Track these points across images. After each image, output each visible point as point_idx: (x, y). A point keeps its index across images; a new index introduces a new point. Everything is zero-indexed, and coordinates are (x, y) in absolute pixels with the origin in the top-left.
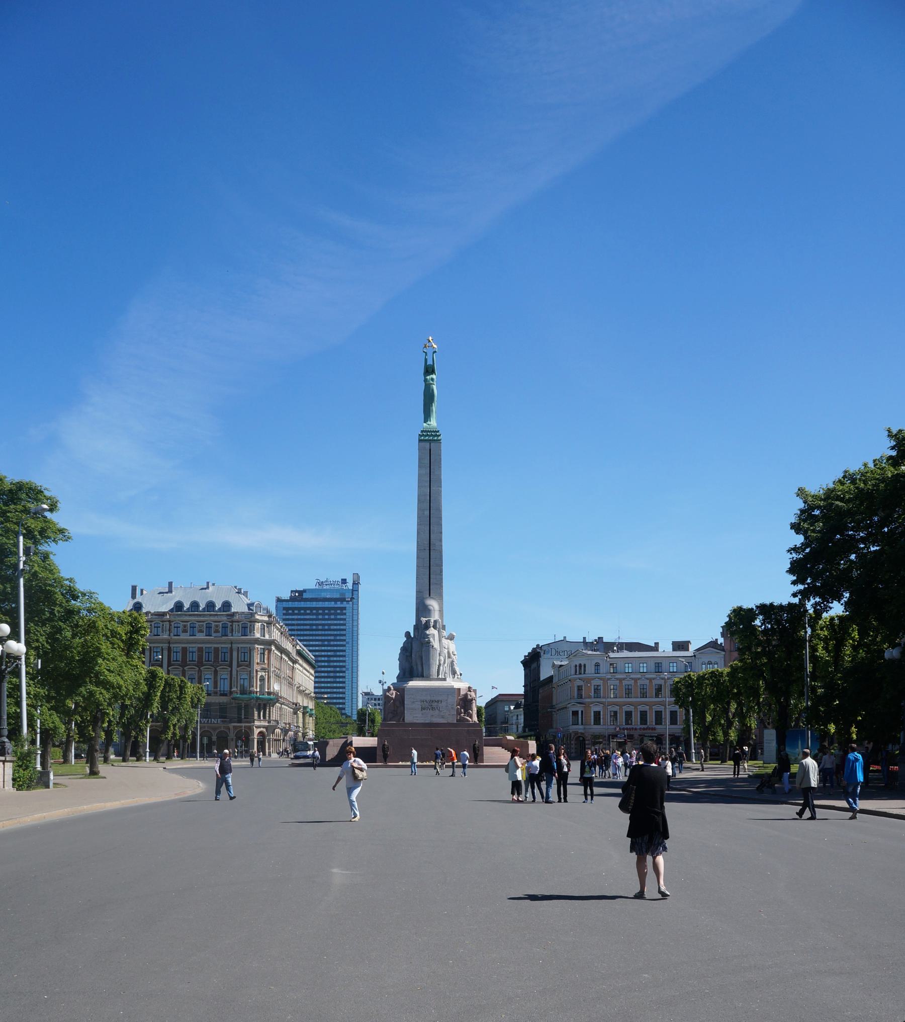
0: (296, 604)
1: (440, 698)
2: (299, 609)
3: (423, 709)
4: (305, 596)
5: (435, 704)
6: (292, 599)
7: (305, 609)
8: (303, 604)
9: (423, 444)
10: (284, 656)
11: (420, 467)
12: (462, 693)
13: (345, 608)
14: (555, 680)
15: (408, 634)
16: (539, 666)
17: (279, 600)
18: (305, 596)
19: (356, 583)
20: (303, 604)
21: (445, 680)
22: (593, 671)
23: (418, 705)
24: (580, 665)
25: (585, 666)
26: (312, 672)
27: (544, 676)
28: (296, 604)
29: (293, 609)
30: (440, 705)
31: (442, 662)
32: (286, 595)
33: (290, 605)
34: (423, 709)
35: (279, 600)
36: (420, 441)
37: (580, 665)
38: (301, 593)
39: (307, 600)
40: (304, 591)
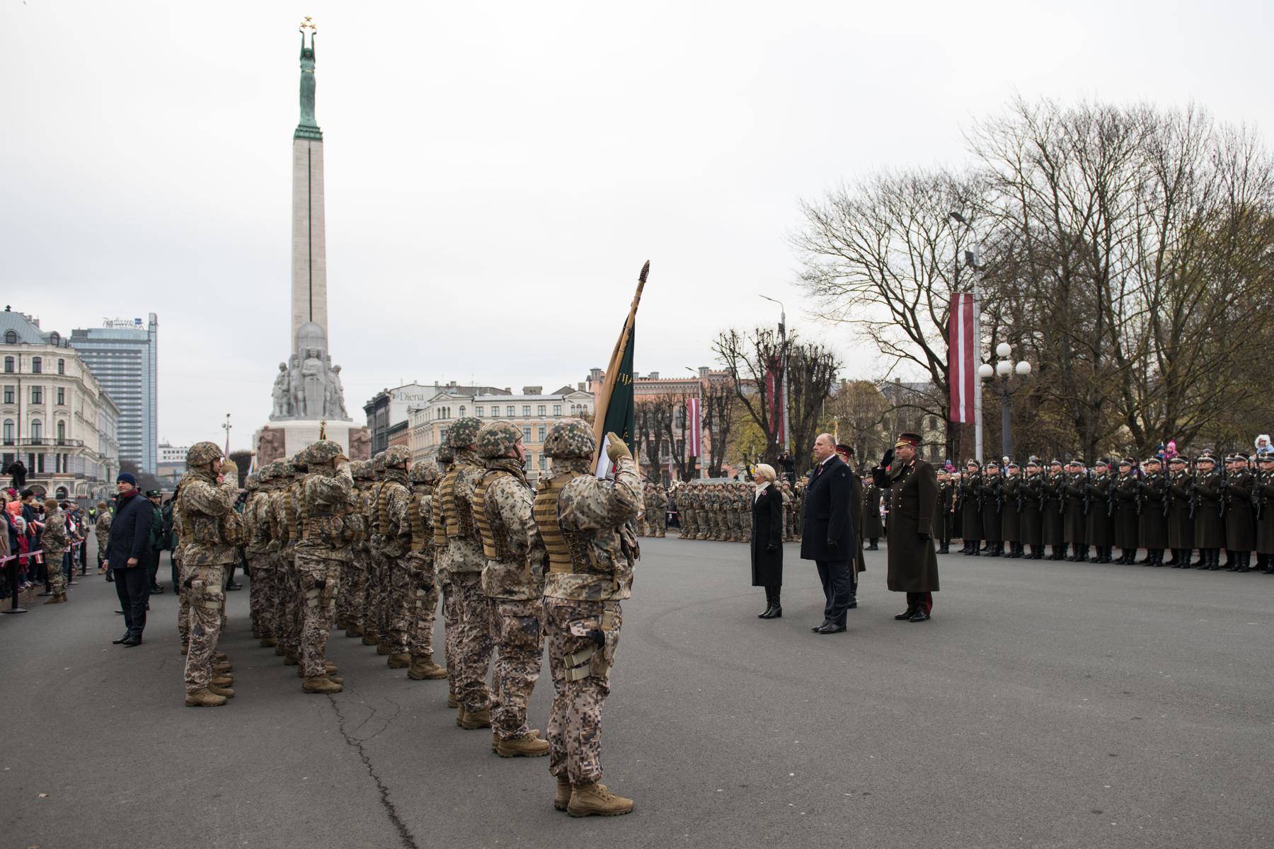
4: (90, 336)
8: (87, 346)
9: (298, 141)
13: (140, 351)
14: (411, 425)
15: (283, 368)
16: (387, 412)
18: (90, 336)
19: (154, 324)
20: (87, 346)
27: (394, 420)
36: (297, 137)
39: (92, 341)
40: (89, 331)
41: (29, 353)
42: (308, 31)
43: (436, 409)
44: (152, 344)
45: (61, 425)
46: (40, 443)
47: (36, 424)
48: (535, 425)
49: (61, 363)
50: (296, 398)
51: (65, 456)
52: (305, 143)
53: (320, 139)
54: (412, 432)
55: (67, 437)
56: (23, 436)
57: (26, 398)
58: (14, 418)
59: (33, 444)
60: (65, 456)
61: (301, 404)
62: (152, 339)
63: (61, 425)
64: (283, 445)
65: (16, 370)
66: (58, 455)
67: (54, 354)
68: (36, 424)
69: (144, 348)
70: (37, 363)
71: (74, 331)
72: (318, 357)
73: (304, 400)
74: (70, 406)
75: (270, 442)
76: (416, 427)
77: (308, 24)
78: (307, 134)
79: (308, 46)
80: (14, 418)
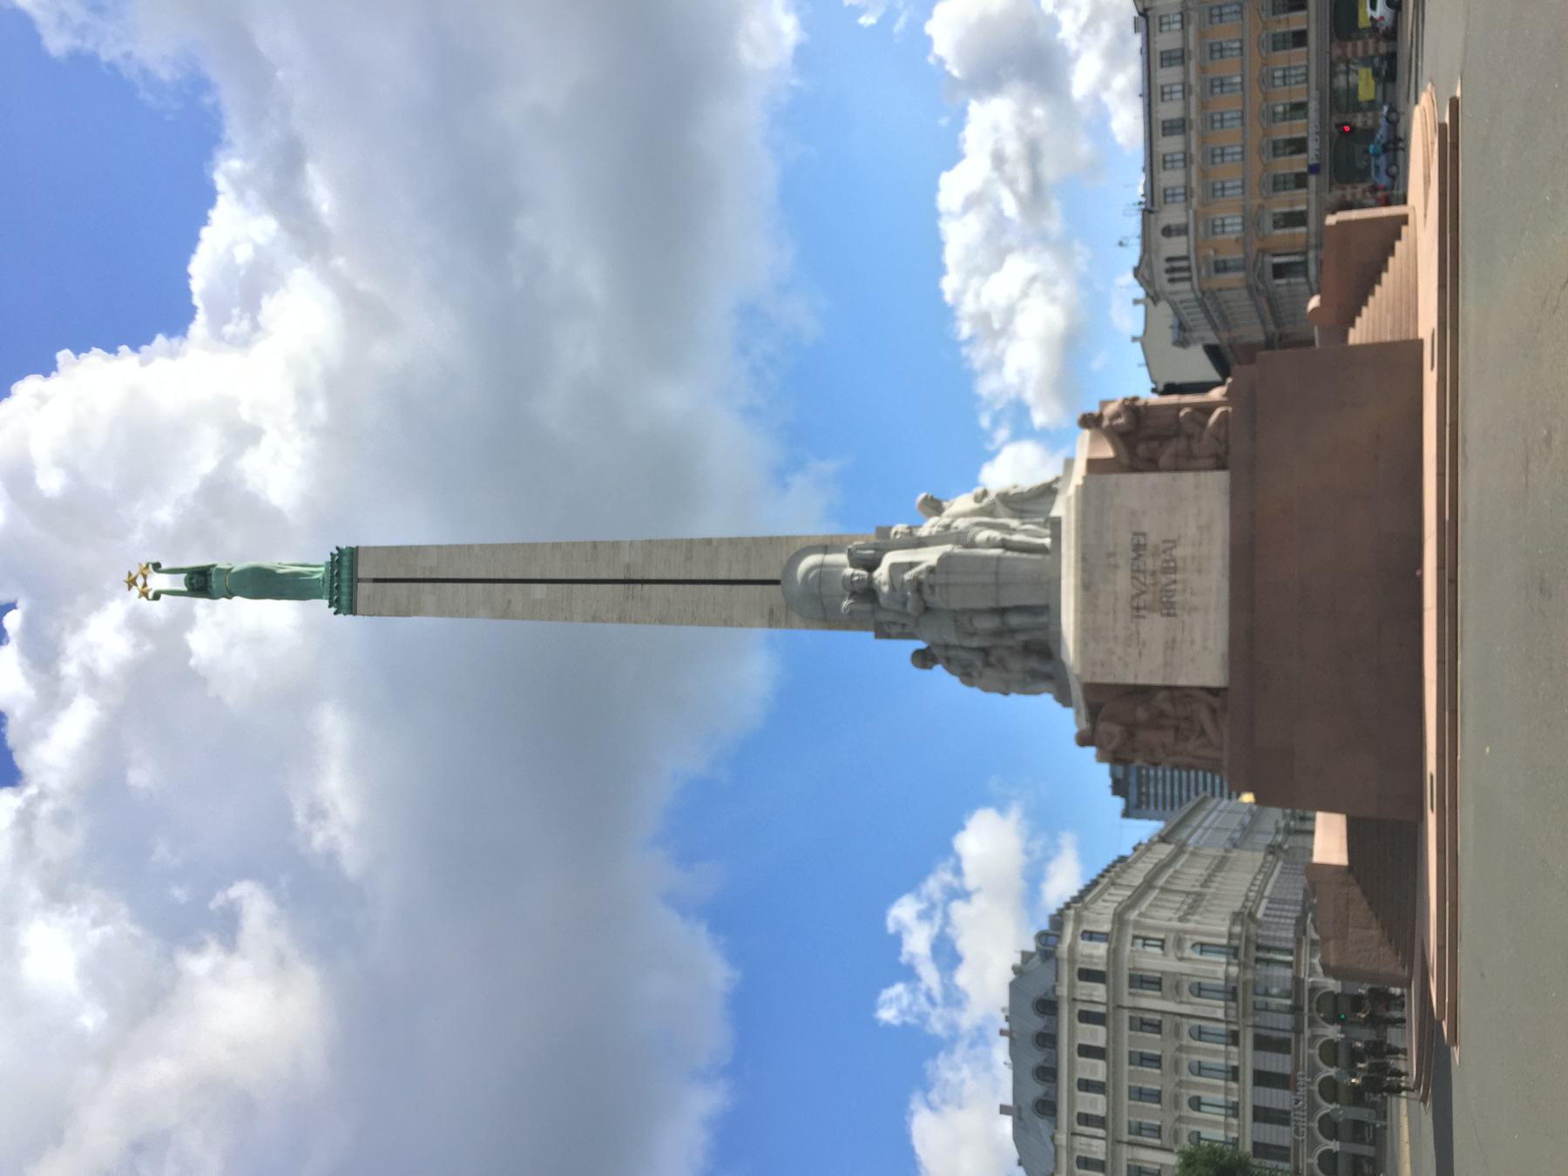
0: (1133, 790)
1: (1125, 539)
10: (1161, 882)
11: (417, 612)
12: (1107, 452)
14: (1212, 339)
15: (924, 659)
17: (1126, 814)
21: (1055, 524)
22: (1183, 239)
23: (1155, 626)
24: (1167, 271)
25: (1169, 259)
26: (1213, 802)
31: (997, 535)
32: (1118, 803)
34: (1168, 608)
35: (1126, 814)
36: (352, 610)
37: (1170, 270)
41: (1072, 987)
42: (158, 582)
43: (1169, 287)
45: (1203, 947)
46: (1235, 989)
47: (1199, 990)
48: (1202, 70)
49: (1090, 936)
50: (998, 633)
51: (1259, 948)
52: (364, 589)
53: (353, 553)
54: (1225, 335)
55: (1224, 941)
56: (1220, 1014)
57: (1151, 1001)
58: (1187, 1024)
59: (1234, 999)
60: (1259, 948)
61: (1014, 620)
63: (1203, 947)
64: (1141, 693)
65: (1101, 1009)
66: (1258, 960)
67: (1072, 949)
68: (1199, 990)
70: (1088, 975)
72: (872, 565)
73: (1002, 612)
74: (1168, 930)
75: (1131, 729)
76: (1215, 328)
77: (140, 581)
78: (345, 589)
79: (179, 583)
80: (1187, 1024)
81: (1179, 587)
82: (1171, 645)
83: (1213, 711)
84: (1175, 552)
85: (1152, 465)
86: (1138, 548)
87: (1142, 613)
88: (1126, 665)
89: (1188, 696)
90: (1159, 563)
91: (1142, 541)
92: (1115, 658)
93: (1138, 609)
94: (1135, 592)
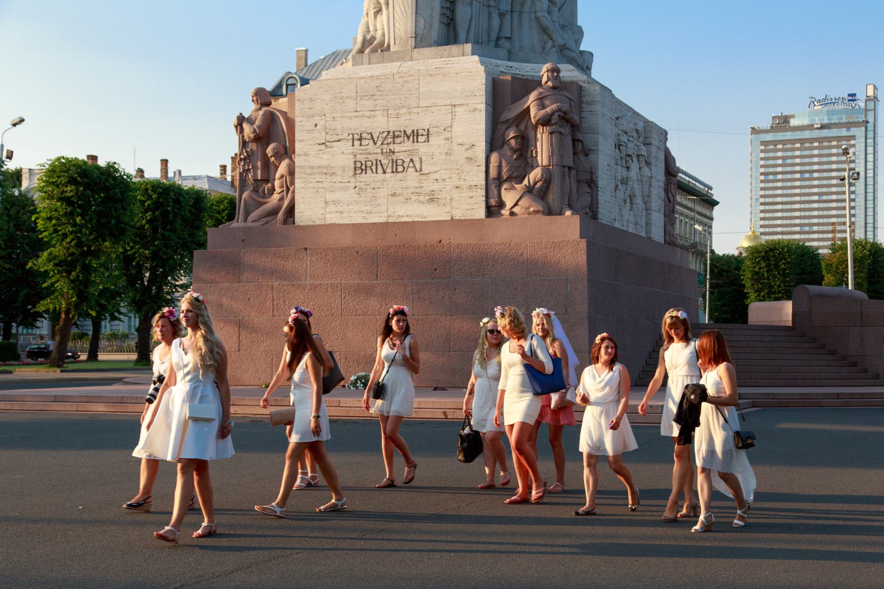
0: (780, 136)
1: (421, 122)
2: (784, 142)
3: (360, 168)
4: (793, 122)
5: (402, 148)
6: (773, 129)
7: (793, 142)
8: (788, 135)
13: (853, 137)
18: (793, 122)
20: (788, 135)
23: (342, 156)
28: (780, 136)
29: (775, 143)
30: (423, 148)
33: (769, 137)
34: (360, 168)
38: (786, 119)
40: (793, 116)
44: (870, 126)
62: (871, 119)
69: (859, 132)
71: (774, 118)
81: (380, 176)
82: (328, 171)
83: (274, 212)
84: (411, 170)
85: (494, 143)
86: (415, 135)
87: (357, 143)
88: (309, 131)
89: (288, 190)
90: (401, 156)
91: (421, 139)
92: (316, 119)
93: (360, 139)
94: (375, 136)
